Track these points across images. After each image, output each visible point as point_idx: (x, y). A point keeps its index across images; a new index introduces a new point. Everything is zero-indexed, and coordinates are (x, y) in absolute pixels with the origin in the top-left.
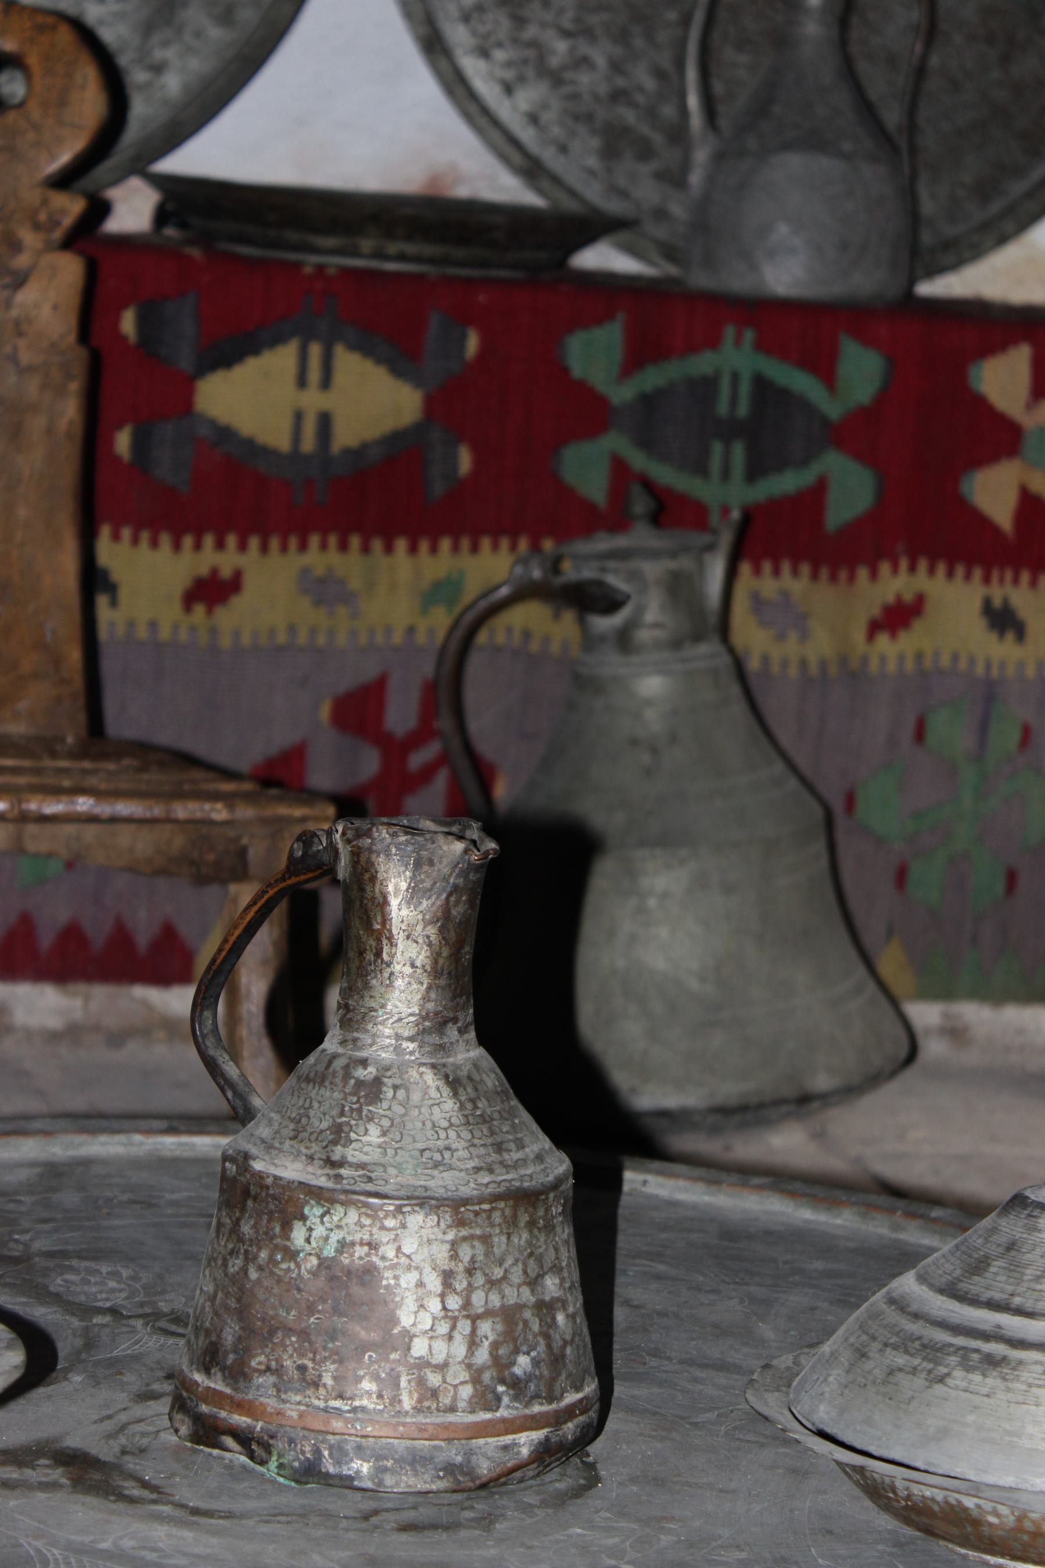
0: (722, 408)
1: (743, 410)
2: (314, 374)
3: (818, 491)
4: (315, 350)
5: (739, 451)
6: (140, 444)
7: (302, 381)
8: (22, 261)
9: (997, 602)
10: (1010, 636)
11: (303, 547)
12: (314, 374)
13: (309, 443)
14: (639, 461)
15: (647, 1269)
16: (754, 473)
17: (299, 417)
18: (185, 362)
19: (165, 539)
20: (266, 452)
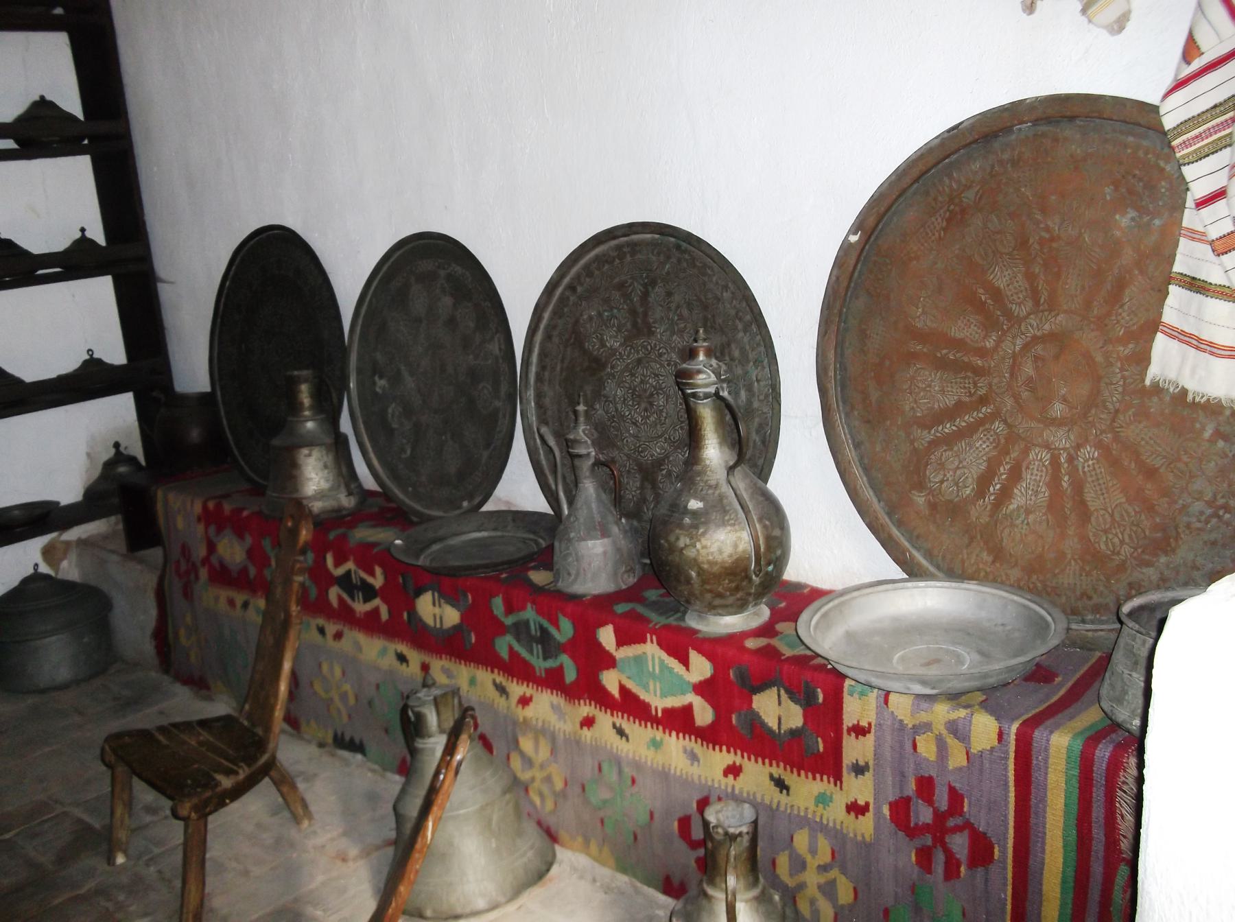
9: (618, 725)
10: (624, 738)
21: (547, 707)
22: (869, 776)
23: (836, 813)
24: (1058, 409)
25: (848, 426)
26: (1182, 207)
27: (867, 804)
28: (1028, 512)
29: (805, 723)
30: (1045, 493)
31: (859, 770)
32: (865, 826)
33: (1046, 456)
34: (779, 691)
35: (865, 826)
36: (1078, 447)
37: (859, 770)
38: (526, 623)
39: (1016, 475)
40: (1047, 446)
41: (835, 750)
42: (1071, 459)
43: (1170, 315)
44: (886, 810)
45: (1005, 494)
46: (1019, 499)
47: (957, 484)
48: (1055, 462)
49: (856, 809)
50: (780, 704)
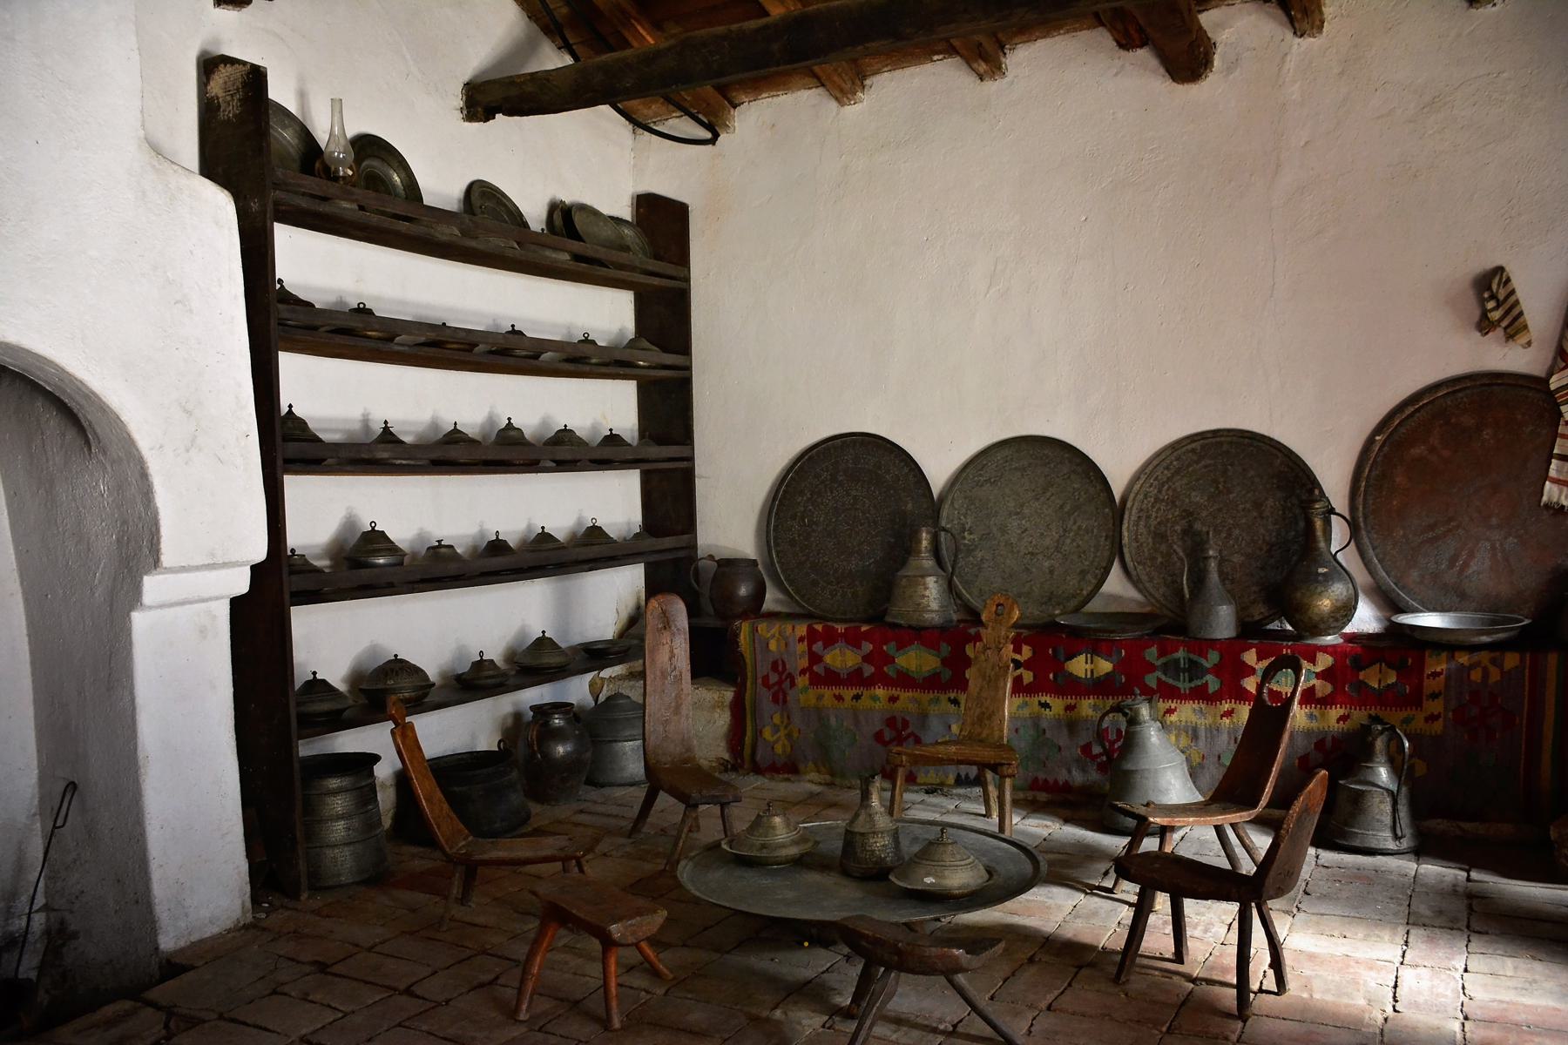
0: (1182, 666)
1: (1187, 666)
2: (1089, 661)
3: (1207, 683)
4: (1089, 655)
5: (1186, 674)
6: (1054, 677)
7: (1086, 663)
8: (1001, 646)
11: (1089, 698)
12: (1089, 661)
13: (1089, 676)
14: (1163, 678)
15: (613, 821)
16: (1191, 680)
17: (1086, 670)
18: (1062, 659)
19: (1061, 697)
20: (1080, 678)
21: (1190, 711)
22: (1441, 698)
23: (1419, 723)
24: (1494, 521)
25: (1369, 538)
26: (1558, 425)
27: (1440, 713)
28: (1479, 574)
29: (1397, 679)
30: (1488, 563)
31: (1434, 696)
32: (1438, 727)
33: (1488, 545)
34: (1381, 665)
35: (1438, 727)
36: (1506, 538)
37: (1434, 696)
38: (1177, 661)
39: (1471, 555)
40: (1488, 539)
41: (1418, 689)
42: (1501, 545)
43: (1552, 473)
44: (1450, 715)
45: (1466, 565)
46: (1473, 567)
47: (1437, 563)
48: (1493, 548)
49: (1432, 718)
50: (1380, 672)
